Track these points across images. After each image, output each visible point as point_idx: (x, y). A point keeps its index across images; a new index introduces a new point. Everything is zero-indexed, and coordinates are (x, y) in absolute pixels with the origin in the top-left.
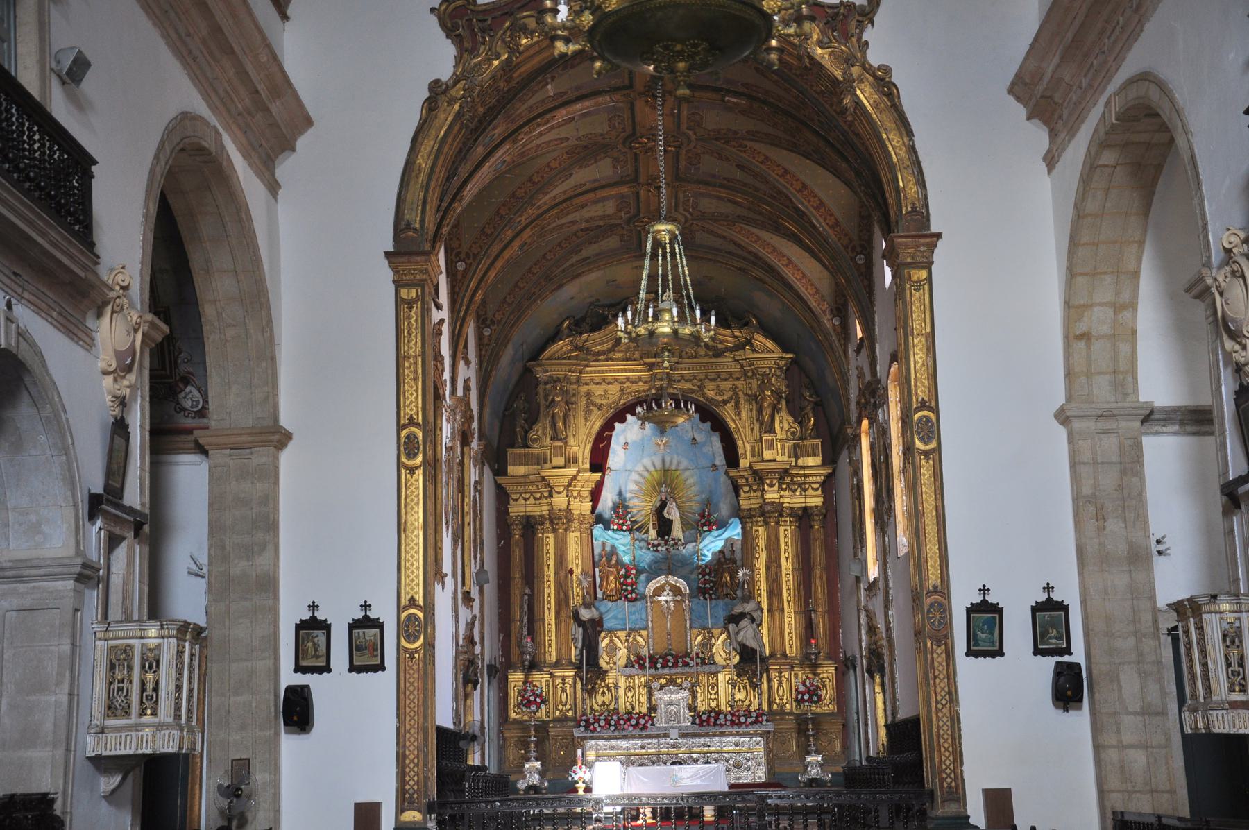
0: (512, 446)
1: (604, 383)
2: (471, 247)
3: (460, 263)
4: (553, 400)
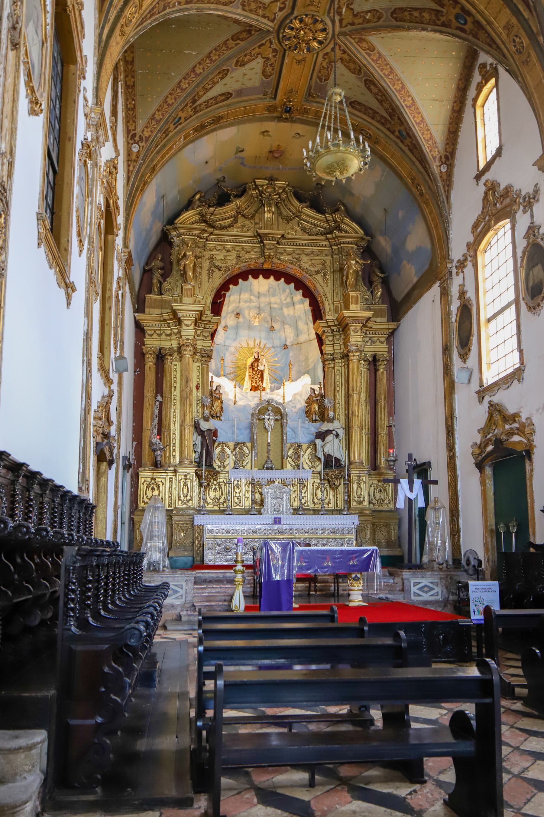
0: (150, 292)
1: (224, 251)
4: (185, 255)
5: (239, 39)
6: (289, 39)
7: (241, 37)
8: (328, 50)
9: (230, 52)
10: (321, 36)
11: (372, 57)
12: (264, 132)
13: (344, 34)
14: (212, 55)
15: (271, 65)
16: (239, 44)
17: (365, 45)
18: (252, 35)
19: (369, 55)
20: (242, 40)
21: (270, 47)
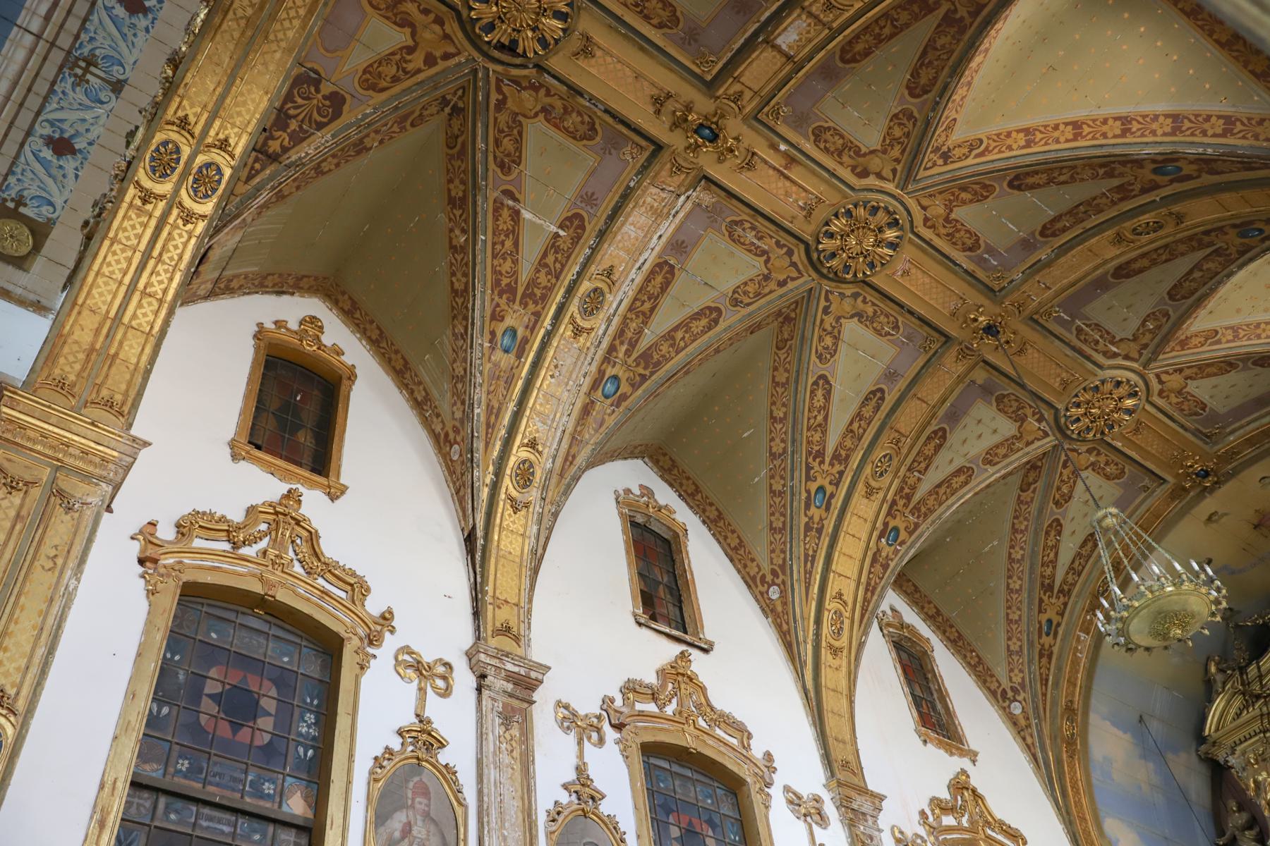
2: (772, 559)
3: (771, 589)
5: (1030, 484)
6: (1088, 429)
7: (1031, 480)
8: (1156, 386)
9: (1034, 507)
10: (1122, 391)
11: (1224, 340)
12: (1210, 519)
13: (1149, 361)
14: (1016, 527)
15: (1107, 463)
16: (1035, 489)
17: (1195, 341)
18: (1041, 467)
19: (1219, 342)
20: (1036, 482)
21: (1079, 454)
